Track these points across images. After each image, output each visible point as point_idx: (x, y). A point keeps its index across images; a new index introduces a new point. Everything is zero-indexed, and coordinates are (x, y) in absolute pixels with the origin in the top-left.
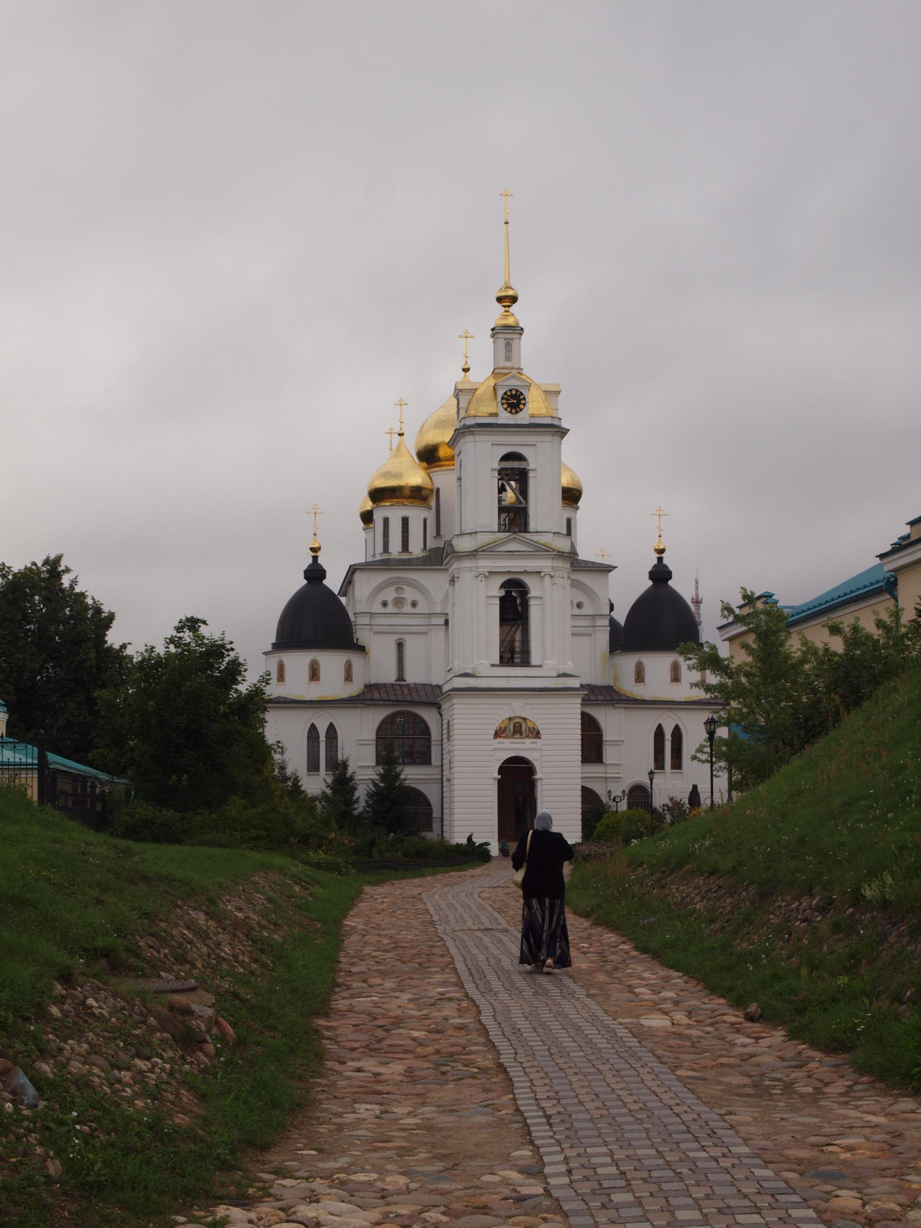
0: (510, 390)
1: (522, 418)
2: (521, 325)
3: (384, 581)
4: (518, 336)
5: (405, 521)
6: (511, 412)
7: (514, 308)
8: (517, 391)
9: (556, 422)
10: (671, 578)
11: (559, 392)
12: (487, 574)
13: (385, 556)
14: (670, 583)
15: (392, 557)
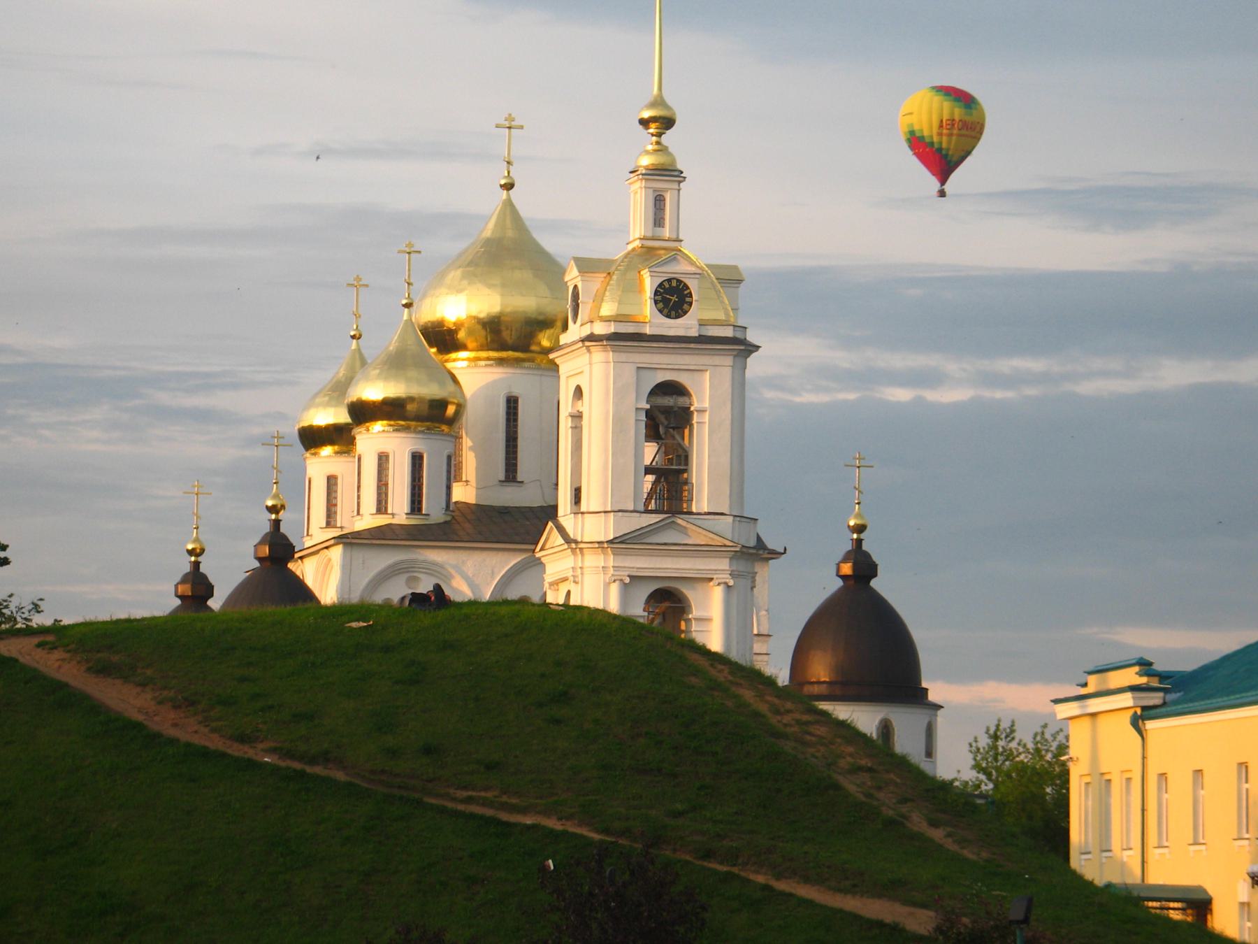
0: (669, 280)
1: (685, 326)
2: (679, 167)
3: (390, 567)
4: (675, 186)
5: (417, 459)
6: (668, 316)
7: (669, 138)
8: (679, 281)
9: (739, 335)
10: (875, 575)
11: (740, 281)
12: (627, 580)
13: (382, 520)
14: (874, 583)
15: (395, 521)
